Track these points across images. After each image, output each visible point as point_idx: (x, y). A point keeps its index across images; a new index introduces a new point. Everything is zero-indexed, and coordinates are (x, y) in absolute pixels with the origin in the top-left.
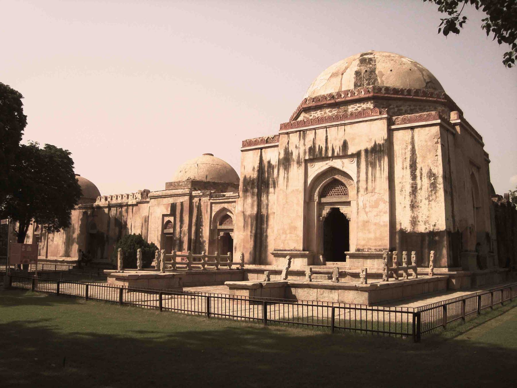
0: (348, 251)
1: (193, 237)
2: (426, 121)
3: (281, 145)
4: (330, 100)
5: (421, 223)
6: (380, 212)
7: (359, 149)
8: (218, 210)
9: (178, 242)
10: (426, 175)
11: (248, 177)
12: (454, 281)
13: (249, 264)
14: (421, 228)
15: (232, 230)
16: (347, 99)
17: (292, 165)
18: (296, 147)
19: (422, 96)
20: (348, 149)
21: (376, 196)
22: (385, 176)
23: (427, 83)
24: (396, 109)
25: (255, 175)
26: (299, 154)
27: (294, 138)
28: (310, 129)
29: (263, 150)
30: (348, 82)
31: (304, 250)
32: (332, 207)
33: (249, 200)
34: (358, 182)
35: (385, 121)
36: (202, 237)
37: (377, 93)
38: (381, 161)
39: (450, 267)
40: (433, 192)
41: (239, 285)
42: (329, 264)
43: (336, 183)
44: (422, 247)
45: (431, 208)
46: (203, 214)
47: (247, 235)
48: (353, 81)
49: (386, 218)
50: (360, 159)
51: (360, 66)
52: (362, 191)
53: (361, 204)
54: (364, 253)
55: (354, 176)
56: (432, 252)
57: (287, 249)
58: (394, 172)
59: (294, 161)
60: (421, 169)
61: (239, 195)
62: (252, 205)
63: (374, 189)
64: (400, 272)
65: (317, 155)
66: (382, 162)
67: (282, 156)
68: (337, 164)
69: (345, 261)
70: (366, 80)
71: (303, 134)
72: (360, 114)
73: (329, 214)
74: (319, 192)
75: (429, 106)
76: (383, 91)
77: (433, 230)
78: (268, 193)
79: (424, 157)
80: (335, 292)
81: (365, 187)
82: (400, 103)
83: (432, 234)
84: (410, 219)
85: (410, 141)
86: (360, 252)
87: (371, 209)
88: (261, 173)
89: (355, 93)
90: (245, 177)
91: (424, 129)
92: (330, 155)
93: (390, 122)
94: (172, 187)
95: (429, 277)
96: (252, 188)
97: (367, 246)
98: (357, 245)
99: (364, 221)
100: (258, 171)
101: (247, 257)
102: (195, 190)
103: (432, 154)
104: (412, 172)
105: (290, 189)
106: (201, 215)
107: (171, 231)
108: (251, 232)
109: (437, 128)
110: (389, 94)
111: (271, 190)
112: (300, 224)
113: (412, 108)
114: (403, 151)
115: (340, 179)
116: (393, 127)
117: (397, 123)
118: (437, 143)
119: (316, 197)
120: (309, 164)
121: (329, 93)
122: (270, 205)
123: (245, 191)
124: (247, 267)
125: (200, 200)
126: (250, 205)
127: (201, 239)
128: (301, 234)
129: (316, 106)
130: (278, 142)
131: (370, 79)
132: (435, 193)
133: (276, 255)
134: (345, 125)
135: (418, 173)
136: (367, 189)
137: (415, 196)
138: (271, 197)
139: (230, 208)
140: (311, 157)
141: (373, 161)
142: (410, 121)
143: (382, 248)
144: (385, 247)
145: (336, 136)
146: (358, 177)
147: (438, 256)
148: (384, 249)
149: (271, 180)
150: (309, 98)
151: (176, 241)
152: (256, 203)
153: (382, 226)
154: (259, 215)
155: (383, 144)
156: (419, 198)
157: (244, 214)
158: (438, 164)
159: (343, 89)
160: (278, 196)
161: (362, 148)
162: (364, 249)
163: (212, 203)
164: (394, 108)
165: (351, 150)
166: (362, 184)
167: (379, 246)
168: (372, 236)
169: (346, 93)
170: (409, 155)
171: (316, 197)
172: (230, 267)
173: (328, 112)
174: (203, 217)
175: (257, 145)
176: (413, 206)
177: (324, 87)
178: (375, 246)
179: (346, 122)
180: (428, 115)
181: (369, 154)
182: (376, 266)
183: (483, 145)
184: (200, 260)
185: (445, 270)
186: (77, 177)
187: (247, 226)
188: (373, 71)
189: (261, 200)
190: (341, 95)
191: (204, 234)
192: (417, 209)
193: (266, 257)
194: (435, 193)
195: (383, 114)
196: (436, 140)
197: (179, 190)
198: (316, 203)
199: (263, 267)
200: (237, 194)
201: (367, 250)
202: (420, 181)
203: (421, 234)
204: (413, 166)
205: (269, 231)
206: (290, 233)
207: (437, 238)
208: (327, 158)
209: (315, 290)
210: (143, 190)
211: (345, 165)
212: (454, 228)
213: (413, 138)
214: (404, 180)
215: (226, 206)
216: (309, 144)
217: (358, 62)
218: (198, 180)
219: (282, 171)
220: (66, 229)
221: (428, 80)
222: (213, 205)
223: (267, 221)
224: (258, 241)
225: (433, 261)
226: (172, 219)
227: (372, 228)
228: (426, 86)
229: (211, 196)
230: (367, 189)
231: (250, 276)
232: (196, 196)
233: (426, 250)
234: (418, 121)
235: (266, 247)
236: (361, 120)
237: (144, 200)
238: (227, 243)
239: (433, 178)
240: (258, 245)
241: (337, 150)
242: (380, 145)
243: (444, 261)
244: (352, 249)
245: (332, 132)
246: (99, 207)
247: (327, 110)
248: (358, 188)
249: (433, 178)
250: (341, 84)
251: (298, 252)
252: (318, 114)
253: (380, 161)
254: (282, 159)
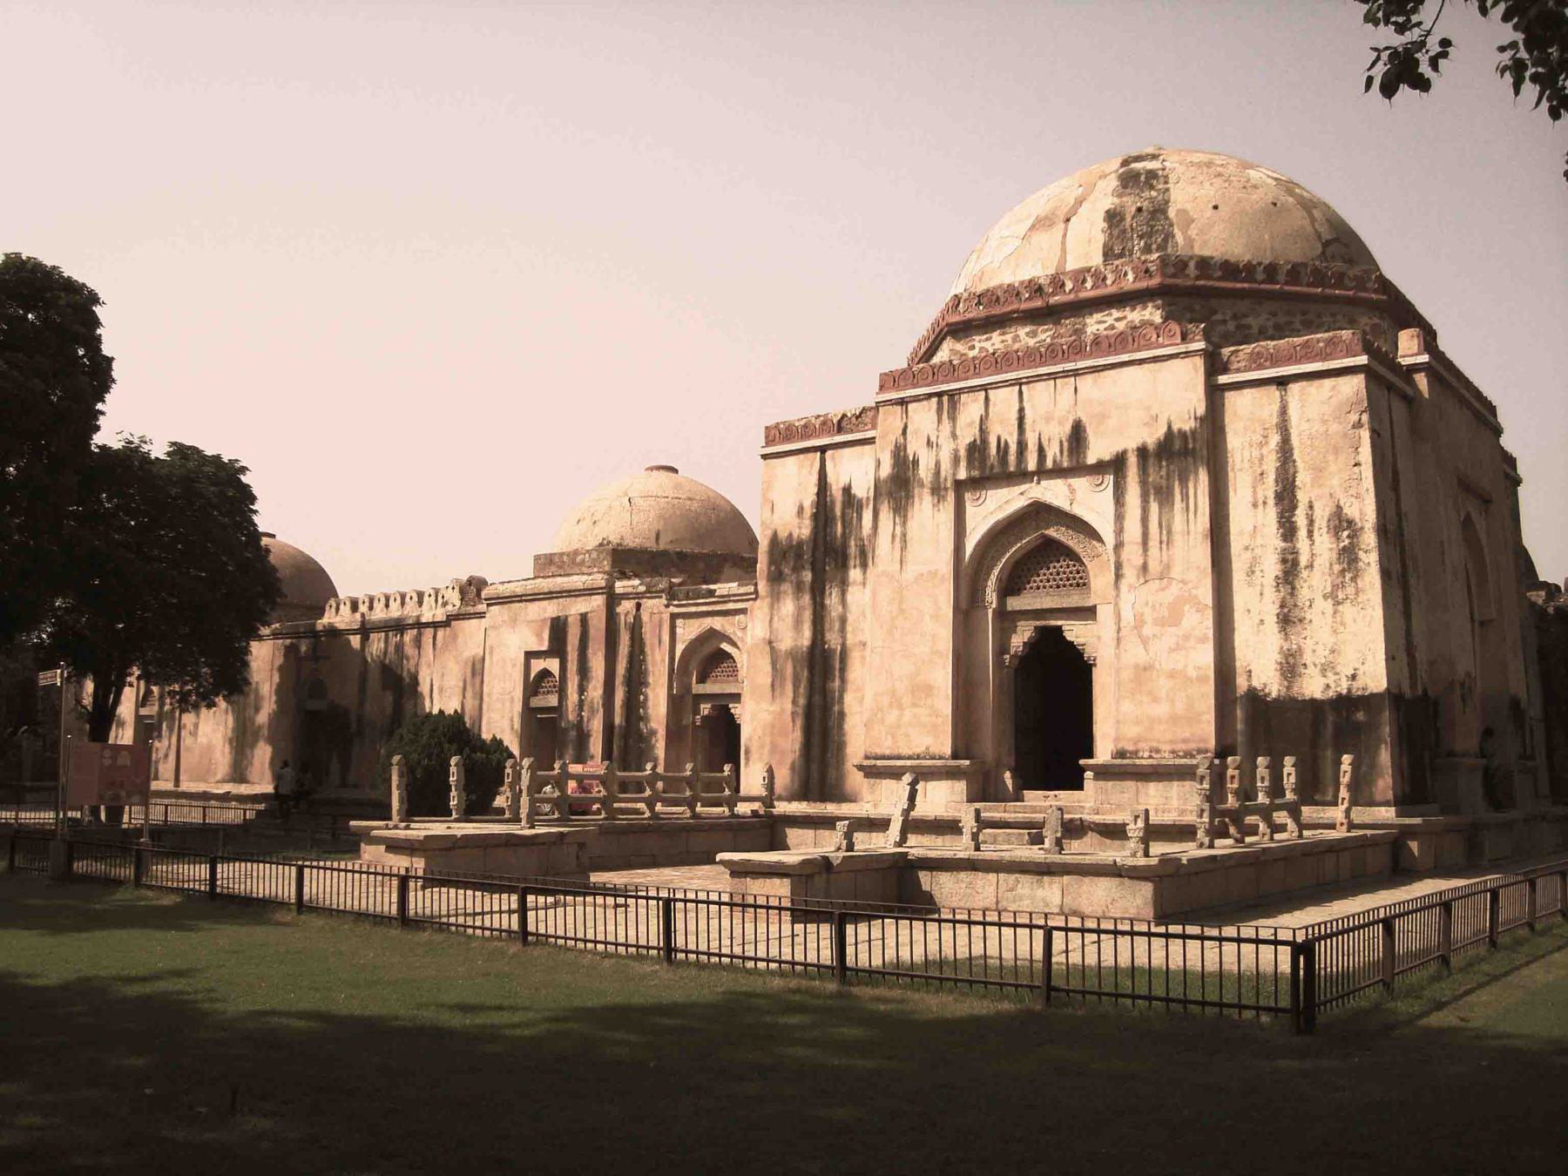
0: (1091, 756)
1: (618, 720)
2: (1324, 360)
3: (883, 437)
4: (1030, 299)
5: (1311, 670)
6: (1187, 637)
7: (1120, 448)
8: (693, 636)
9: (573, 733)
10: (1324, 524)
11: (783, 535)
12: (1414, 845)
13: (790, 799)
14: (1313, 686)
15: (736, 697)
16: (1083, 295)
18: (929, 443)
19: (1309, 285)
20: (1086, 447)
21: (1175, 589)
22: (1200, 529)
23: (1326, 244)
24: (1231, 326)
25: (804, 530)
26: (938, 464)
27: (923, 417)
28: (972, 389)
29: (829, 453)
30: (1085, 245)
31: (955, 756)
32: (1038, 623)
33: (788, 606)
34: (1119, 546)
35: (1199, 362)
36: (645, 719)
37: (1174, 276)
38: (1187, 481)
39: (1403, 802)
40: (1348, 576)
41: (761, 864)
42: (1034, 797)
43: (1051, 551)
44: (1314, 745)
45: (1343, 624)
46: (648, 649)
47: (783, 710)
48: (1100, 239)
49: (1205, 657)
50: (1124, 477)
51: (1120, 196)
52: (1130, 574)
53: (1128, 616)
54: (1138, 762)
55: (1106, 529)
56: (1347, 759)
57: (905, 751)
58: (1226, 518)
59: (922, 485)
60: (1311, 507)
61: (756, 592)
62: (798, 623)
63: (1168, 567)
64: (1250, 819)
66: (1191, 485)
67: (886, 470)
68: (1053, 492)
69: (1081, 788)
70: (1141, 237)
71: (949, 402)
72: (1120, 342)
74: (999, 579)
75: (1333, 315)
76: (1192, 270)
77: (1349, 690)
78: (844, 584)
79: (1318, 471)
80: (1051, 883)
82: (1243, 306)
83: (1346, 704)
84: (1278, 658)
85: (1275, 420)
86: (1126, 762)
87: (1157, 630)
88: (821, 525)
89: (1104, 279)
90: (775, 534)
91: (1317, 383)
92: (1032, 465)
93: (1215, 365)
94: (553, 568)
95: (1340, 833)
96: (797, 569)
97: (1146, 740)
98: (1117, 739)
99: (1136, 666)
100: (815, 517)
101: (783, 779)
102: (624, 576)
103: (1342, 458)
104: (1281, 515)
105: (911, 570)
106: (642, 652)
107: (553, 701)
108: (794, 702)
109: (1357, 383)
110: (1209, 278)
111: (854, 574)
112: (942, 677)
113: (1282, 319)
114: (1256, 453)
115: (1063, 539)
116: (1223, 379)
117: (1235, 366)
118: (1358, 425)
119: (991, 596)
120: (968, 496)
121: (1027, 277)
122: (851, 618)
123: (776, 578)
124: (782, 808)
125: (638, 606)
126: (790, 621)
127: (642, 725)
128: (946, 707)
129: (987, 318)
130: (874, 427)
131: (1150, 235)
132: (1354, 579)
133: (872, 773)
134: (1076, 373)
135: (1300, 518)
137: (1293, 588)
138: (853, 594)
139: (729, 631)
140: (976, 473)
141: (1164, 483)
142: (1275, 361)
143: (1193, 746)
144: (1202, 745)
145: (1048, 410)
146: (1119, 531)
147: (1364, 768)
148: (1199, 751)
149: (853, 543)
150: (965, 295)
151: (565, 731)
152: (807, 615)
153: (1190, 679)
154: (817, 652)
155: (1193, 432)
156: (1304, 593)
157: (772, 649)
158: (1363, 492)
159: (1071, 265)
160: (874, 594)
161: (1130, 443)
162: (1136, 752)
163: (674, 617)
164: (1224, 322)
165: (1096, 451)
166: (1132, 554)
167: (1184, 741)
168: (1162, 710)
169: (1080, 276)
170: (1271, 465)
171: (991, 596)
172: (731, 810)
173: (1024, 337)
174: (649, 658)
175: (809, 437)
176: (1287, 620)
177: (1012, 258)
178: (1171, 742)
179: (1081, 364)
180: (1329, 342)
181: (1151, 461)
182: (1175, 803)
183: (1497, 431)
184: (643, 791)
185: (1387, 814)
186: (265, 541)
187: (782, 686)
188: (1160, 210)
189: (823, 606)
190: (1063, 285)
191: (650, 711)
192: (1299, 628)
193: (841, 777)
194: (1354, 579)
195: (1193, 340)
196: (1354, 417)
197: (575, 578)
198: (990, 612)
199: (831, 809)
200: (752, 589)
201: (1146, 755)
202: (1307, 542)
203: (1313, 701)
204: (1286, 496)
205: (849, 698)
206: (915, 705)
207: (1360, 716)
208: (1022, 476)
209: (992, 877)
210: (465, 578)
211: (1079, 495)
212: (1413, 686)
213: (1283, 411)
214: (1259, 541)
215: (717, 623)
216: (968, 435)
217: (1113, 182)
218: (632, 545)
219: (886, 516)
220: (235, 698)
221: (1327, 236)
222: (679, 622)
223: (843, 670)
224: (817, 727)
225: (1350, 787)
226: (553, 665)
227: (1163, 685)
228: (1323, 253)
229: (672, 595)
230: (1145, 567)
231: (793, 834)
232: (626, 596)
233: (1329, 753)
234: (1299, 362)
235: (841, 746)
236: (1125, 357)
237: (471, 609)
238: (723, 737)
239: (1346, 533)
240: (816, 740)
241: (1052, 452)
243: (1384, 784)
244: (1103, 752)
245: (1040, 398)
246: (332, 632)
247: (1023, 331)
248: (1118, 566)
249: (1346, 533)
250: (1064, 250)
251: (939, 763)
252: (995, 342)
253: (1184, 482)
254: (885, 481)
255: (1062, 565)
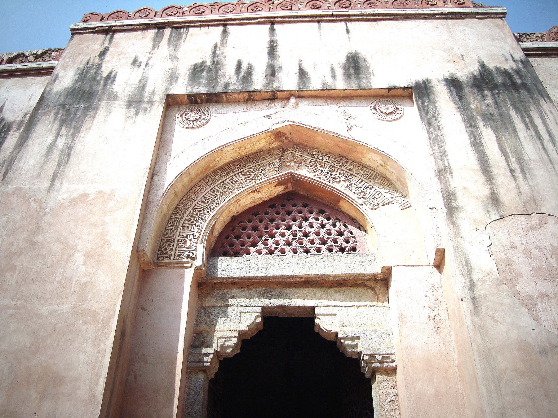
17: (101, 112)
34: (443, 173)
59: (114, 97)
65: (227, 85)
73: (249, 342)
81: (485, 191)
134: (347, 19)
136: (494, 199)
140: (202, 90)
141: (493, 110)
155: (518, 72)
181: (468, 91)
198: (189, 275)
208: (273, 97)
230: (494, 199)
242: (506, 73)
254: (59, 94)
255: (314, 224)
